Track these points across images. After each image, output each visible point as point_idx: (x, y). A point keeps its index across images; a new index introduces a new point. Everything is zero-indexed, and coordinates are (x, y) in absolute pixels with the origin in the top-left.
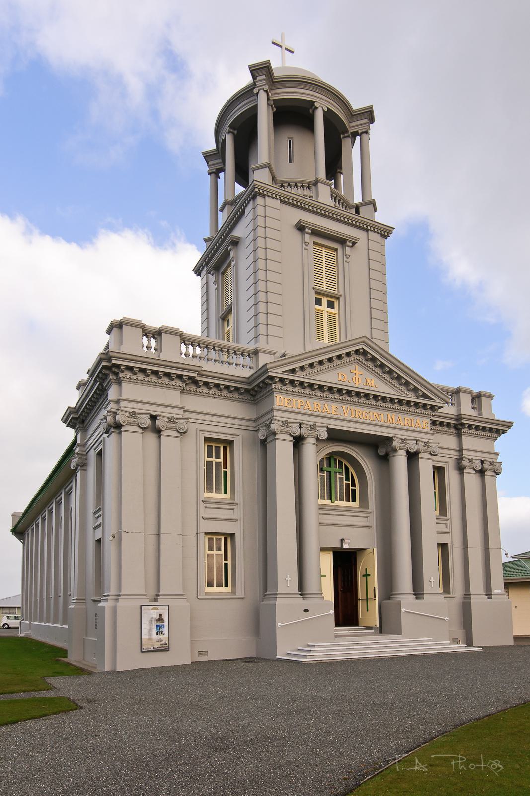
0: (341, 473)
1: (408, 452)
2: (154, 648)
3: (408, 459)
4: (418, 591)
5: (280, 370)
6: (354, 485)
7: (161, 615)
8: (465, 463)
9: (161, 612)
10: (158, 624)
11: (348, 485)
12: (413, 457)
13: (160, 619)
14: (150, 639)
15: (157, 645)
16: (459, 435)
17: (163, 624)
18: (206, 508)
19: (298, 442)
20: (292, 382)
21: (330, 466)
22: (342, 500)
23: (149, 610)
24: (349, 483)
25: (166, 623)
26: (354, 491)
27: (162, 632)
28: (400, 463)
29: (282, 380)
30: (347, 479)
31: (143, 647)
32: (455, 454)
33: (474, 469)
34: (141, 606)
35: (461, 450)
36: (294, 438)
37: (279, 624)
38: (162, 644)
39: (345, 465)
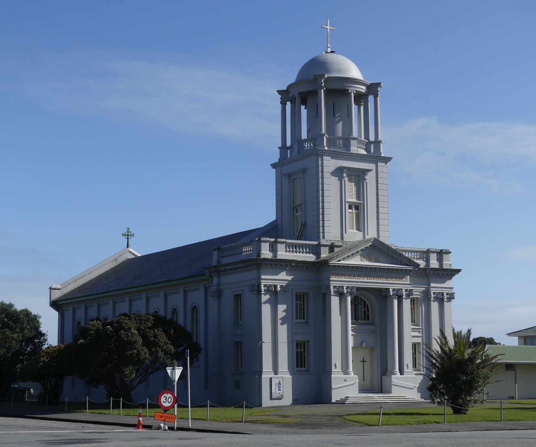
0: (361, 305)
6: (368, 310)
7: (280, 382)
9: (280, 380)
11: (365, 311)
12: (400, 298)
13: (280, 384)
14: (275, 393)
15: (278, 395)
22: (362, 320)
23: (275, 379)
24: (365, 310)
25: (282, 385)
26: (368, 314)
27: (280, 389)
30: (365, 308)
31: (273, 396)
38: (280, 395)
39: (363, 299)
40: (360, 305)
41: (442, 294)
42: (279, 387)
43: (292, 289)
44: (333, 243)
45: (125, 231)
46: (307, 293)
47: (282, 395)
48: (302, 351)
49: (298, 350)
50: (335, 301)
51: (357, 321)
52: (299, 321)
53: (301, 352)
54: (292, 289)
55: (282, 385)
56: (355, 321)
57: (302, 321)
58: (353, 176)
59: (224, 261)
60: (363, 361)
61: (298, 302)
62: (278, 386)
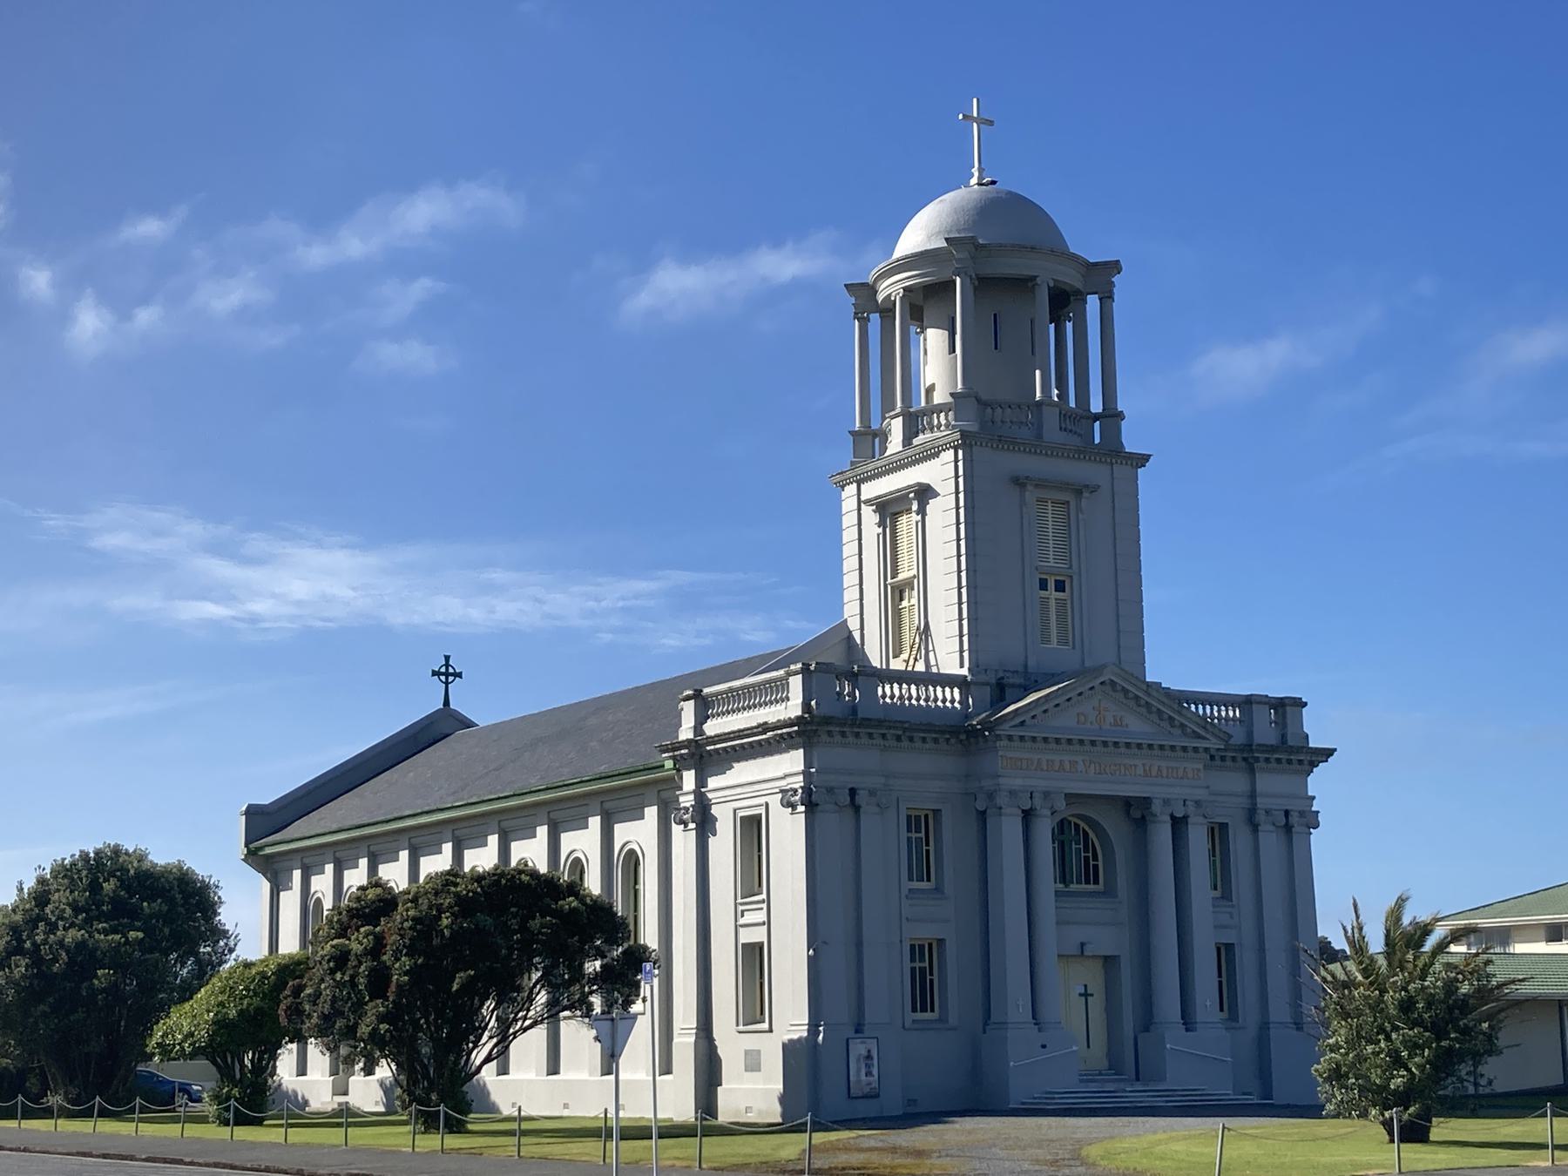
1: (1173, 817)
3: (1173, 826)
4: (1188, 1022)
6: (1095, 858)
7: (869, 1051)
8: (1261, 817)
11: (1086, 859)
12: (1179, 824)
15: (867, 1090)
16: (1252, 771)
19: (1028, 816)
20: (1022, 738)
21: (1063, 834)
22: (1079, 882)
25: (875, 1062)
26: (1096, 867)
28: (1162, 835)
29: (1010, 738)
30: (1086, 850)
31: (852, 1091)
32: (1244, 802)
33: (1274, 824)
35: (1253, 795)
36: (1023, 811)
37: (1012, 1064)
38: (871, 1089)
39: (1084, 830)
40: (1073, 843)
41: (1287, 813)
43: (898, 799)
44: (1003, 678)
45: (438, 664)
46: (937, 812)
47: (875, 1088)
48: (925, 968)
49: (914, 965)
50: (1009, 830)
51: (1066, 886)
52: (916, 885)
53: (922, 970)
54: (898, 799)
55: (875, 1062)
56: (1062, 886)
57: (924, 885)
58: (1050, 504)
59: (713, 727)
60: (1086, 995)
61: (914, 835)
62: (866, 1065)
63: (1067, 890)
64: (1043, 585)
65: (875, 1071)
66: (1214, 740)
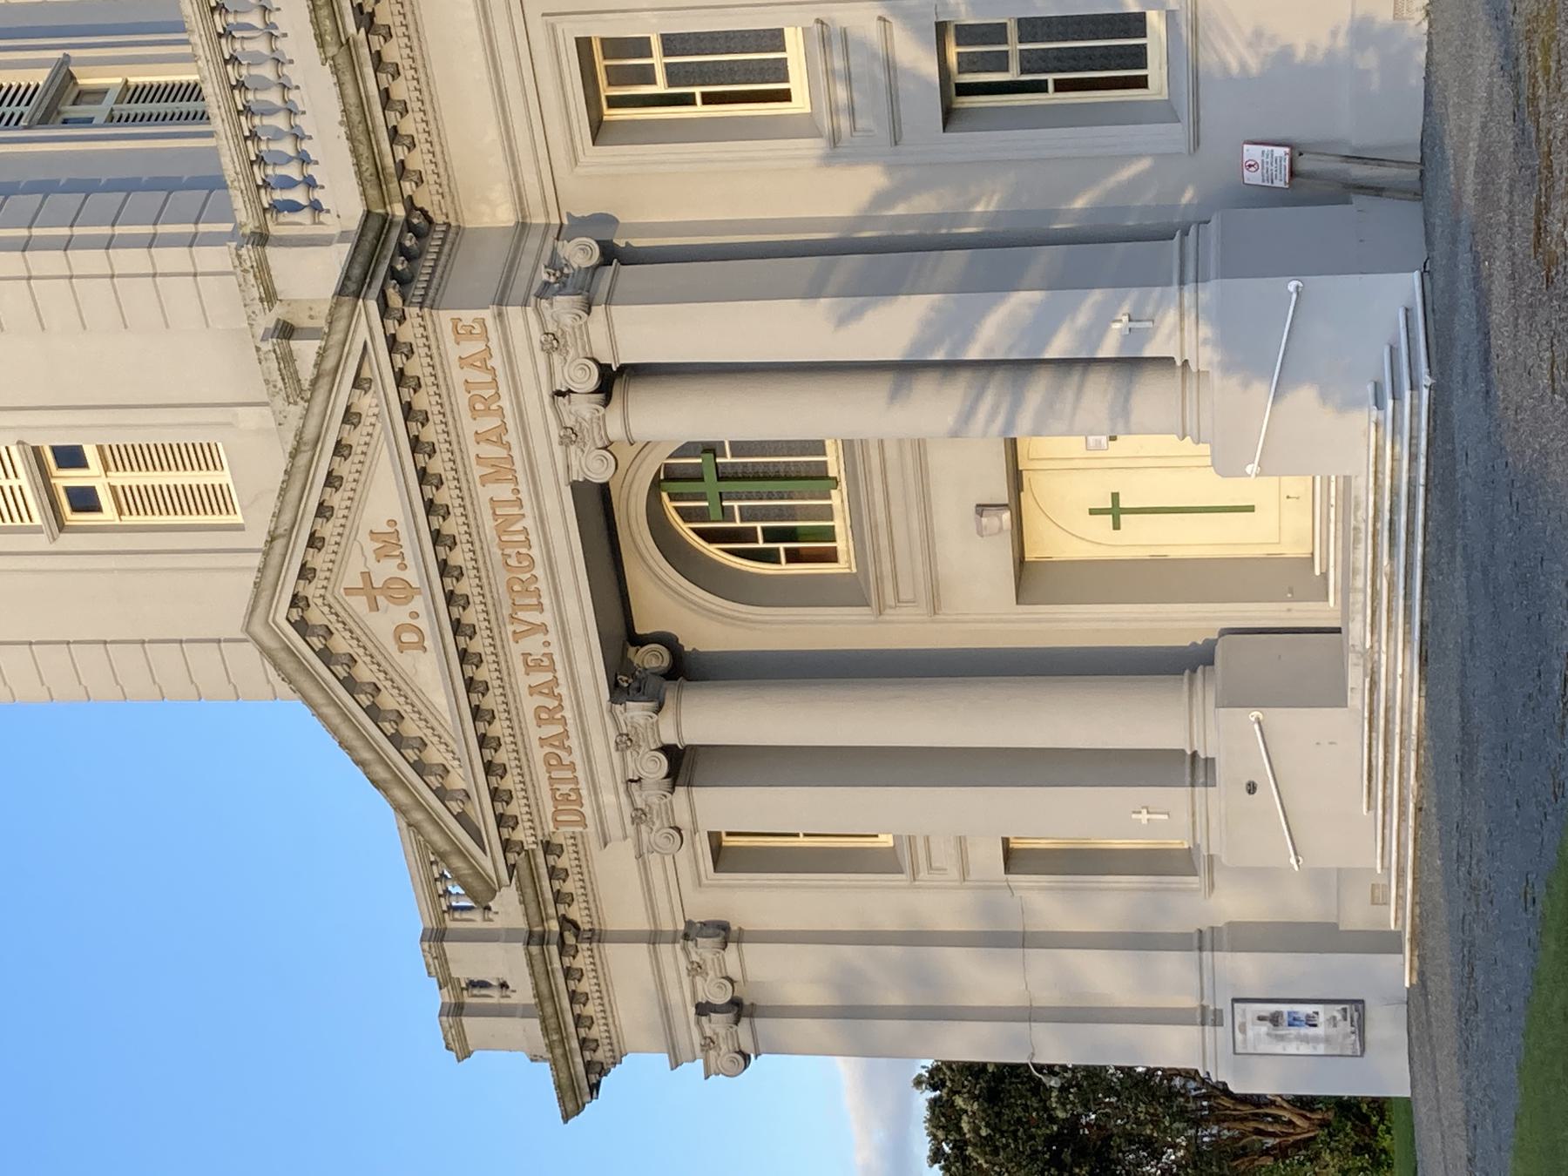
2: (1353, 1033)
5: (486, 863)
7: (1261, 1019)
10: (1286, 1023)
15: (1345, 1027)
17: (1286, 1016)
18: (930, 867)
27: (1308, 1017)
34: (1235, 1053)
42: (1294, 1021)
47: (1345, 1010)
55: (1285, 1008)
62: (1290, 1025)
63: (843, 483)
64: (85, 500)
65: (1308, 1009)
66: (362, 334)
